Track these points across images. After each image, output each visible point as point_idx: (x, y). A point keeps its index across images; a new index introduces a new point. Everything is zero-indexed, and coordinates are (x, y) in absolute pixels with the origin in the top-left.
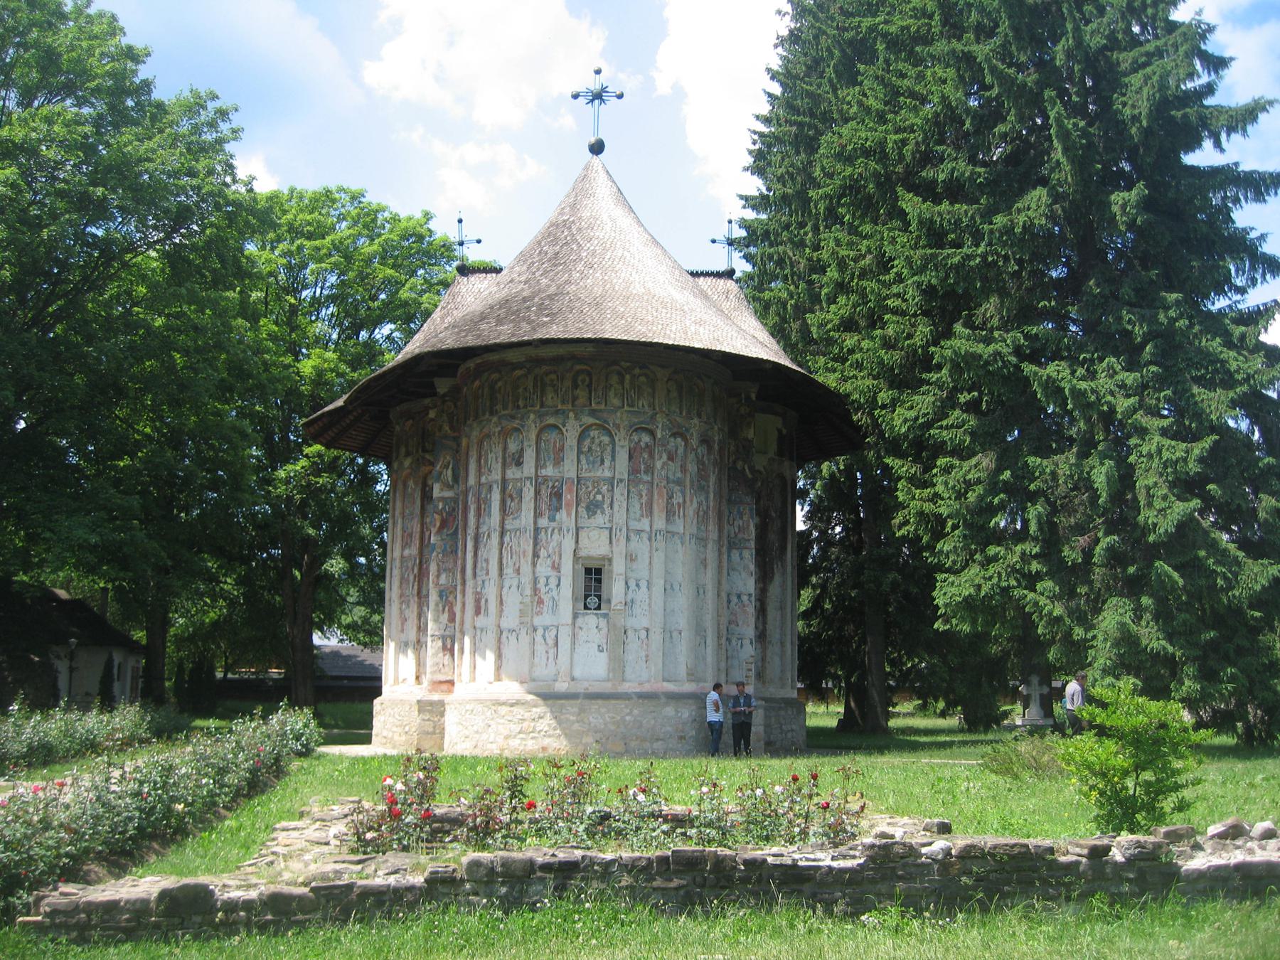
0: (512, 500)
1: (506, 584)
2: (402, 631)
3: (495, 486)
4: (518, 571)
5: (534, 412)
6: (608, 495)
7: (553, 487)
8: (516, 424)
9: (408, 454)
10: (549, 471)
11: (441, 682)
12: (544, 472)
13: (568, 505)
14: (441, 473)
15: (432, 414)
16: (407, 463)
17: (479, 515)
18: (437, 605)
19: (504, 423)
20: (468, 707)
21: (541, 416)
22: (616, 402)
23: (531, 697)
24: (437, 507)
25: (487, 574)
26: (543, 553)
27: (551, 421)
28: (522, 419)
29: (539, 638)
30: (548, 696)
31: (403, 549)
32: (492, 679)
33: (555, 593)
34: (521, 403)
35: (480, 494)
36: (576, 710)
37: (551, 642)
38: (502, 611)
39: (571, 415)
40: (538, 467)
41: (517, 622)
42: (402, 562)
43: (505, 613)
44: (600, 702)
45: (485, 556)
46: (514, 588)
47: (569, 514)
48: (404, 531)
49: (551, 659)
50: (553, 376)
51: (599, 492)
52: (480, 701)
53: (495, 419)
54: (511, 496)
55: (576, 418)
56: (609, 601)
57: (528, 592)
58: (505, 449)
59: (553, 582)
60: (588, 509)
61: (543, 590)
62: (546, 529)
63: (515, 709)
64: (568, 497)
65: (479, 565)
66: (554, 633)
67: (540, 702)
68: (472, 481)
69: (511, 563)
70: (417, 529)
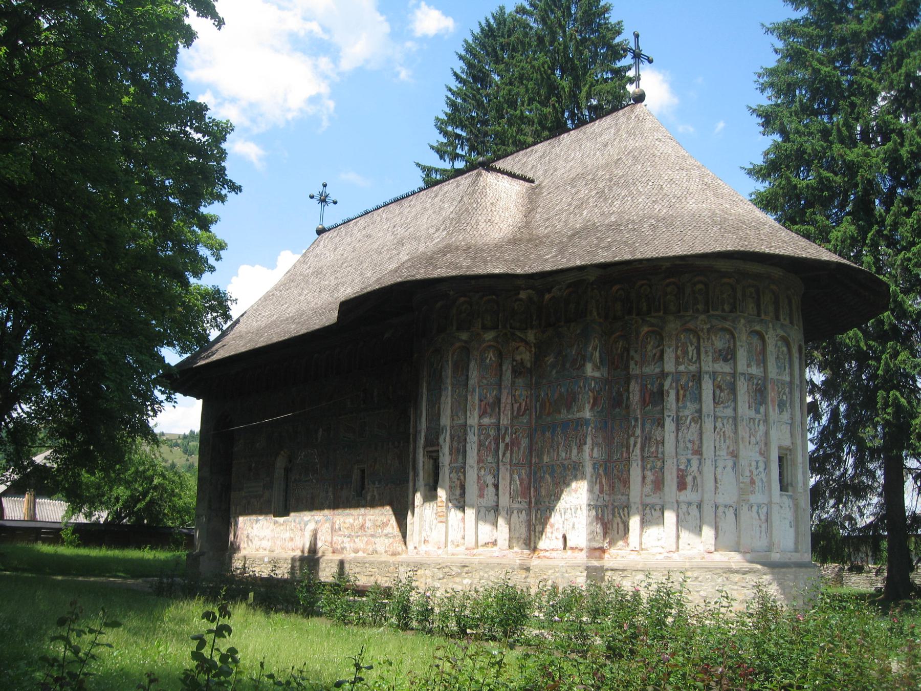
0: (722, 391)
1: (721, 464)
2: (481, 496)
3: (706, 377)
4: (735, 455)
5: (744, 318)
6: (789, 396)
7: (757, 384)
8: (727, 325)
9: (485, 328)
10: (754, 370)
11: (595, 549)
12: (749, 369)
13: (773, 401)
14: (592, 354)
15: (523, 295)
16: (489, 336)
17: (678, 400)
18: (592, 477)
22: (788, 320)
23: (759, 567)
24: (590, 385)
25: (699, 452)
26: (753, 440)
27: (758, 328)
28: (733, 321)
29: (755, 515)
30: (772, 566)
31: (480, 417)
32: (712, 549)
33: (763, 475)
34: (727, 307)
35: (677, 381)
36: (792, 577)
37: (763, 518)
38: (716, 488)
39: (770, 325)
40: (749, 366)
41: (735, 498)
42: (479, 430)
43: (719, 490)
44: (804, 570)
45: (689, 436)
46: (729, 469)
47: (774, 410)
48: (481, 401)
49: (763, 533)
50: (752, 290)
51: (784, 393)
52: (708, 569)
53: (702, 317)
54: (719, 387)
55: (774, 330)
56: (792, 485)
57: (748, 474)
58: (713, 345)
59: (762, 466)
60: (779, 406)
61: (755, 473)
62: (754, 419)
63: (748, 577)
64: (771, 395)
65: (681, 445)
66: (765, 510)
67: (765, 569)
68: (669, 366)
69: (724, 446)
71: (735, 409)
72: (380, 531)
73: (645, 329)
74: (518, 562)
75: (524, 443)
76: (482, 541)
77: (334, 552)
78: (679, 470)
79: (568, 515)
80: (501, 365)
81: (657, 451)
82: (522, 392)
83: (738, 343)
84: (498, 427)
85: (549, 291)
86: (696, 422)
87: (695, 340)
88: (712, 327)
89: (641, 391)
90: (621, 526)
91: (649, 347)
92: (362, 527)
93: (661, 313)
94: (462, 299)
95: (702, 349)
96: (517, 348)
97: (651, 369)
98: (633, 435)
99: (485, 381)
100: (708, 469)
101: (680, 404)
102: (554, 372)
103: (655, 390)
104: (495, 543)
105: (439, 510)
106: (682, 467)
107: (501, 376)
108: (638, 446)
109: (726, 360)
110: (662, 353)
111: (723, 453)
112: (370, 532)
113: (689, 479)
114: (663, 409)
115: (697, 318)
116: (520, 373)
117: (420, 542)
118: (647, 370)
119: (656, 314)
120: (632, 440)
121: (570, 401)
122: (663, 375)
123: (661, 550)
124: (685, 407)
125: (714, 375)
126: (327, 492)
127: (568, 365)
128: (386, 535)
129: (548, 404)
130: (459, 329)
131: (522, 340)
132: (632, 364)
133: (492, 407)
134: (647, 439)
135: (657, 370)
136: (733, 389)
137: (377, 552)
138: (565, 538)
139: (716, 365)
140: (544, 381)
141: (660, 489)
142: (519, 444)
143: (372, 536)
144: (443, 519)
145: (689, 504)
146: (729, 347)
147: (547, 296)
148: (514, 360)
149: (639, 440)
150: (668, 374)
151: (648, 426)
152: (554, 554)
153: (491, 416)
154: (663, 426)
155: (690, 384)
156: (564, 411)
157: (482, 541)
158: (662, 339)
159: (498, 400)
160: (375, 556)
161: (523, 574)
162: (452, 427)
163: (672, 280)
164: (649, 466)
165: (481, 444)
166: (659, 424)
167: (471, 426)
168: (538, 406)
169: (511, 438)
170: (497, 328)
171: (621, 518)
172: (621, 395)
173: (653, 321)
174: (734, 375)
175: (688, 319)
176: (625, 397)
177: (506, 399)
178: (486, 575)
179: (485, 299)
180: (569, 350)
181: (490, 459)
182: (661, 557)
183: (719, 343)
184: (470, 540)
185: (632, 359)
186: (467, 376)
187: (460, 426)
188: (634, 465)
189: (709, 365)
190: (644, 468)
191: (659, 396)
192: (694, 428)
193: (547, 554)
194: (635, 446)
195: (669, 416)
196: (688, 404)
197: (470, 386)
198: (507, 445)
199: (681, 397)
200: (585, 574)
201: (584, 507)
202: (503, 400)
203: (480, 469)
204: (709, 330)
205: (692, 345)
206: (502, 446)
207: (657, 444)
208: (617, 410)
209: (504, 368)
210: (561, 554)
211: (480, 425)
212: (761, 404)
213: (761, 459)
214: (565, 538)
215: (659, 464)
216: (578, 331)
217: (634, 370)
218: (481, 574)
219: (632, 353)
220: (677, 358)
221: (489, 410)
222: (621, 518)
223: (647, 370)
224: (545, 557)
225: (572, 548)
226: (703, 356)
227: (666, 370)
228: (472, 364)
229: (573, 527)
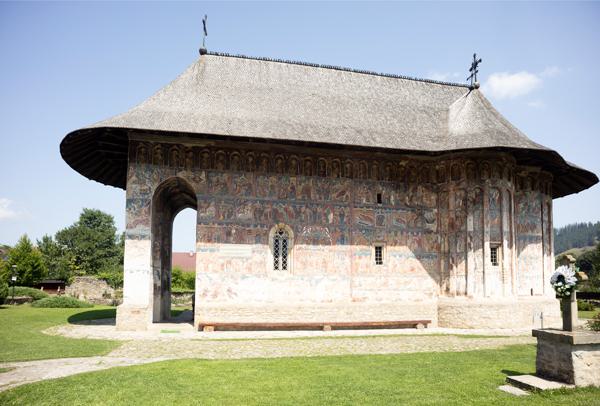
77: (354, 301)
92: (385, 284)
121: (533, 227)
128: (410, 290)
137: (400, 300)
143: (395, 290)
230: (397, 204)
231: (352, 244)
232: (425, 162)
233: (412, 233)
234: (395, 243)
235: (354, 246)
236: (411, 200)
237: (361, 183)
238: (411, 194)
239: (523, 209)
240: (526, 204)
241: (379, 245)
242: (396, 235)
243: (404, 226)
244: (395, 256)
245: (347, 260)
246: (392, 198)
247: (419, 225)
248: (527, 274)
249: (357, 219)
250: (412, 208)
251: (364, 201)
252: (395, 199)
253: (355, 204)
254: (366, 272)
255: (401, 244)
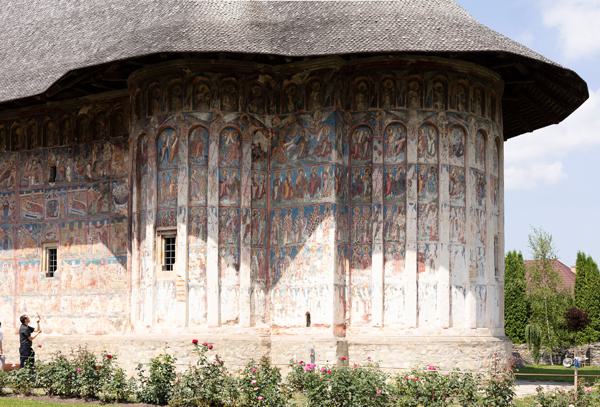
0: (455, 183)
1: (454, 249)
10: (479, 166)
15: (261, 80)
16: (229, 118)
19: (452, 119)
20: (430, 347)
21: (478, 121)
25: (435, 238)
27: (484, 127)
31: (220, 198)
45: (427, 224)
46: (460, 254)
48: (220, 182)
65: (421, 231)
68: (412, 158)
70: (245, 181)
71: (465, 200)
72: (79, 311)
73: (390, 121)
74: (260, 339)
75: (262, 225)
76: (223, 320)
78: (418, 253)
79: (312, 294)
80: (240, 148)
81: (398, 236)
82: (260, 176)
83: (469, 140)
84: (238, 208)
85: (289, 78)
86: (434, 211)
87: (433, 135)
88: (450, 123)
89: (384, 178)
90: (361, 304)
91: (391, 139)
92: (56, 307)
93: (405, 108)
94: (200, 78)
95: (440, 142)
96: (255, 132)
97: (395, 160)
98: (376, 220)
99: (225, 163)
100: (443, 253)
101: (420, 194)
102: (295, 157)
103: (397, 179)
104: (236, 321)
105: (178, 289)
106: (421, 251)
107: (241, 158)
108: (381, 230)
109: (458, 155)
110: (405, 144)
111: (455, 239)
112: (68, 311)
113: (428, 261)
114: (405, 197)
115: (437, 114)
116: (258, 157)
117: (154, 320)
118: (390, 160)
119: (400, 108)
120: (375, 227)
121: (315, 185)
122: (406, 165)
123: (403, 326)
124: (424, 197)
125: (450, 168)
126: (6, 272)
127: (311, 152)
128: (88, 316)
129: (287, 188)
130: (196, 108)
131: (261, 124)
132: (375, 154)
133: (229, 189)
134: (388, 226)
135: (400, 161)
136: (463, 182)
137: (76, 332)
138: (308, 316)
139: (452, 160)
140: (283, 166)
141: (400, 270)
142: (258, 225)
143: (69, 316)
144: (184, 298)
145: (427, 286)
146: (461, 143)
147: (286, 82)
148: (253, 144)
149: (382, 226)
150: (410, 165)
151: (389, 212)
152: (296, 331)
153: (231, 197)
154: (405, 212)
155: (429, 175)
156: (307, 196)
157: (223, 320)
158: (405, 130)
159: (237, 184)
160: (74, 335)
161: (264, 351)
162: (190, 208)
163: (416, 76)
164: (390, 250)
165: (221, 226)
166: (400, 211)
167: (213, 207)
168: (276, 188)
169: (252, 222)
170: (237, 110)
171: (360, 296)
172: (362, 183)
173: (397, 113)
174: (464, 169)
175: (429, 114)
176: (366, 184)
177: (245, 181)
178: (232, 352)
179: (225, 79)
180: (312, 137)
181: (230, 240)
182: (403, 332)
183: (454, 138)
184: (213, 318)
185: (376, 149)
186: (207, 157)
187: (200, 206)
188: (377, 248)
189: (446, 158)
190: (385, 252)
191: (403, 183)
192: (432, 216)
193: (287, 331)
194: (377, 230)
195: (411, 204)
196: (427, 193)
197: (211, 168)
198: (248, 226)
199: (421, 187)
200: (335, 348)
201: (332, 287)
202: (244, 183)
203: (220, 250)
204: (447, 126)
205: (431, 139)
206: (243, 227)
207: (399, 229)
208: (357, 197)
209: (244, 151)
210: (304, 330)
211: (220, 206)
212: (483, 197)
213: (481, 245)
214: (308, 316)
215: (400, 248)
216: (323, 120)
217: (378, 159)
218: (228, 350)
219: (375, 143)
220: (419, 150)
221: (228, 191)
222: (360, 296)
223: (390, 160)
224: (285, 333)
225: (317, 325)
226: (441, 149)
227: (410, 161)
228: (213, 148)
229: (319, 306)
230: (75, 178)
231: (16, 248)
232: (115, 100)
233: (94, 223)
234: (71, 242)
235: (19, 251)
236: (94, 170)
237: (29, 154)
238: (94, 160)
239: (293, 151)
240: (302, 139)
241: (52, 246)
242: (72, 229)
243: (83, 213)
244: (70, 263)
245: (11, 273)
246: (68, 172)
247: (105, 209)
248: (299, 284)
249: (24, 211)
250: (94, 182)
251: (33, 182)
252: (73, 174)
253: (22, 187)
254: (30, 290)
255: (78, 242)
